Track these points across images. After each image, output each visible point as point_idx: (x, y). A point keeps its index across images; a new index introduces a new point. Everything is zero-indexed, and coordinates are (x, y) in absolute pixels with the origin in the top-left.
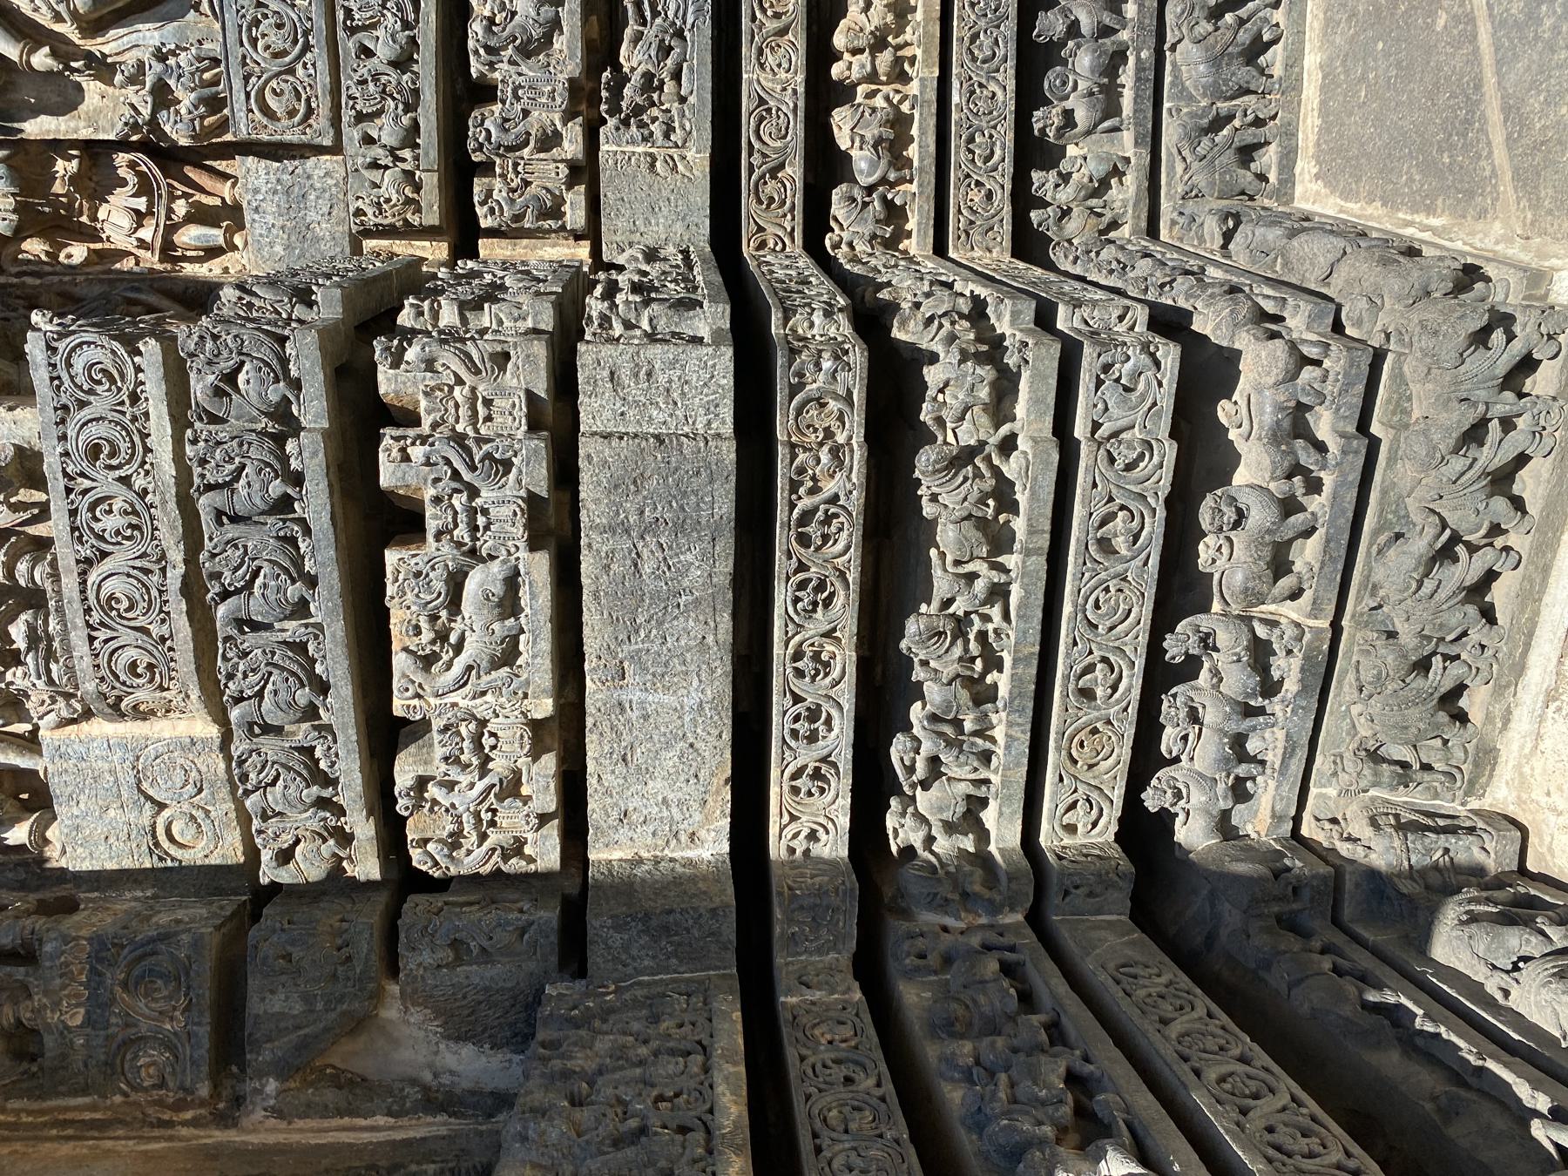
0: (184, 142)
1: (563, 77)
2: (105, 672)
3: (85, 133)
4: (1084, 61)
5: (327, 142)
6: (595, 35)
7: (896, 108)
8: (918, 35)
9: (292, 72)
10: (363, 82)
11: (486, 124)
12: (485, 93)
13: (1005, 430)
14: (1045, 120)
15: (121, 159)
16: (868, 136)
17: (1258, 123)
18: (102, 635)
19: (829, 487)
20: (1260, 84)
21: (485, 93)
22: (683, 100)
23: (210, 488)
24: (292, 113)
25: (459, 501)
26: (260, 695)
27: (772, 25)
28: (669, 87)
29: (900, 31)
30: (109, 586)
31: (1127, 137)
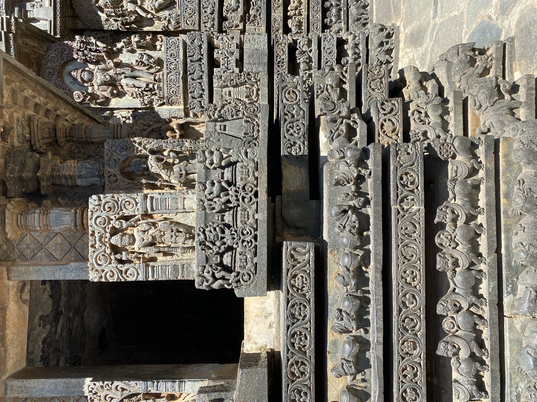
0: (172, 30)
1: (240, 15)
2: (169, 92)
3: (154, 30)
4: (334, 11)
5: (197, 29)
6: (245, 9)
7: (300, 20)
8: (304, 7)
9: (192, 17)
10: (205, 17)
11: (226, 24)
12: (226, 19)
13: (310, 49)
14: (327, 21)
15: (159, 36)
16: (294, 24)
17: (366, 19)
18: (169, 85)
19: (282, 57)
20: (365, 12)
21: (226, 19)
22: (261, 19)
23: (190, 56)
24: (191, 24)
25: (226, 59)
26: (194, 92)
27: (277, 6)
28: (258, 17)
29: (300, 7)
30: (171, 77)
31: (343, 23)
